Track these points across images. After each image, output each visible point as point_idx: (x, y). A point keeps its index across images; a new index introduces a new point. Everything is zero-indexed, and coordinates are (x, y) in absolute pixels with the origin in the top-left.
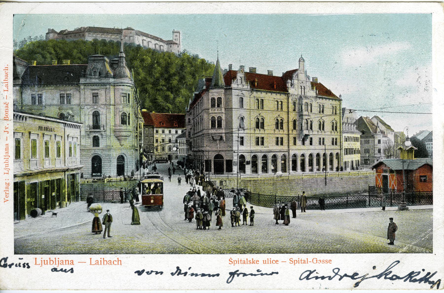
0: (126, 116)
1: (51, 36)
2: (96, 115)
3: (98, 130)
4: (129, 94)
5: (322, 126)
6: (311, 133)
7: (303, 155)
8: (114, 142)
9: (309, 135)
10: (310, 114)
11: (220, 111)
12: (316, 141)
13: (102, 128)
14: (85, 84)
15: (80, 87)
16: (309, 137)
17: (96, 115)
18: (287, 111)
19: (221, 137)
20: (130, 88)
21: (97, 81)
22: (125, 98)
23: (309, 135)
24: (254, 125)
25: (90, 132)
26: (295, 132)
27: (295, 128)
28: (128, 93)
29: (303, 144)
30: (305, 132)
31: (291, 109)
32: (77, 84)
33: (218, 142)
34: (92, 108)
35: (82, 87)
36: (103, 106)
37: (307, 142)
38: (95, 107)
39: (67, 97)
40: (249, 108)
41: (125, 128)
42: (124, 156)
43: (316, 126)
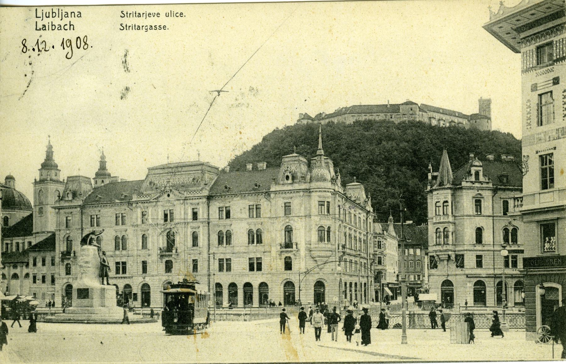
0: (324, 230)
1: (305, 122)
2: (289, 230)
3: (289, 249)
4: (328, 202)
11: (447, 220)
13: (294, 246)
14: (275, 192)
15: (270, 196)
17: (289, 230)
19: (449, 257)
21: (290, 188)
22: (323, 207)
24: (500, 238)
25: (282, 252)
32: (266, 192)
33: (446, 262)
34: (283, 222)
35: (272, 195)
36: (296, 219)
38: (287, 221)
39: (256, 208)
40: (491, 214)
41: (324, 246)
42: (322, 281)
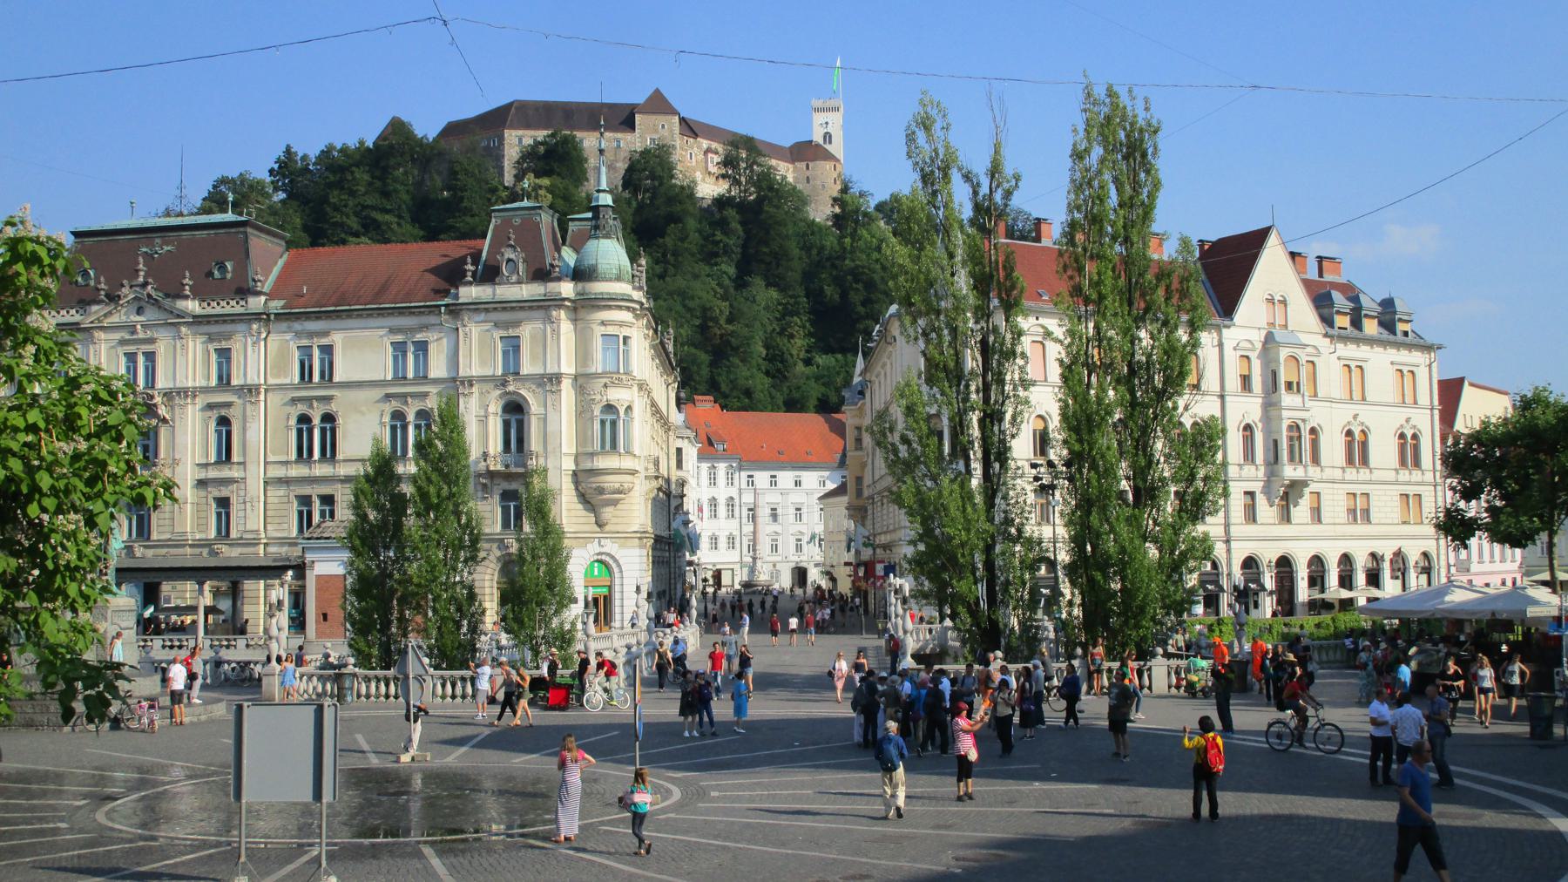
4: (626, 339)
5: (1357, 450)
6: (1313, 472)
7: (1284, 565)
9: (1304, 484)
10: (1309, 404)
12: (1335, 505)
16: (1307, 491)
18: (1217, 389)
20: (627, 316)
23: (1304, 484)
26: (1249, 470)
27: (1249, 455)
28: (625, 332)
29: (1286, 518)
30: (1290, 472)
31: (1233, 383)
37: (1301, 511)
43: (1333, 448)
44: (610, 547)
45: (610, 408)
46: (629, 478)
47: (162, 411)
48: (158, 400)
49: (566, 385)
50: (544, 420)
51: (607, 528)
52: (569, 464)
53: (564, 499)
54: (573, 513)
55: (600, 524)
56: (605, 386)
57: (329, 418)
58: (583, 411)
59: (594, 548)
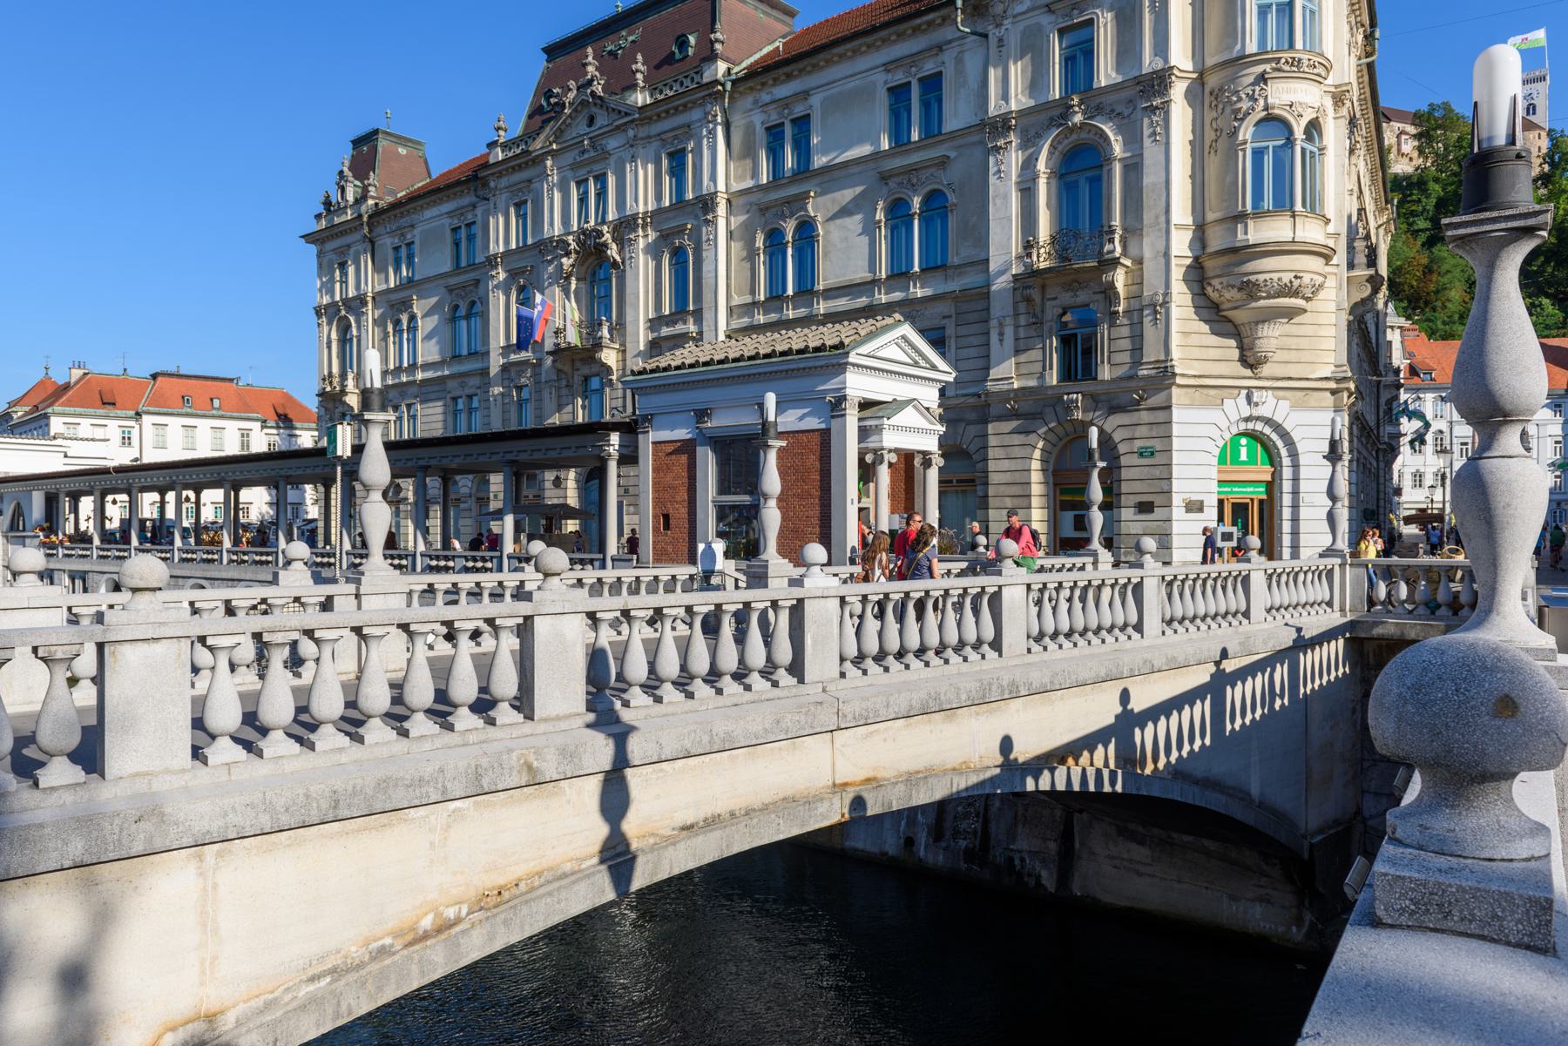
2: (1082, 169)
8: (1189, 342)
44: (1269, 405)
45: (1274, 122)
46: (1315, 263)
47: (613, 252)
48: (607, 237)
49: (1178, 90)
50: (1134, 168)
51: (1266, 370)
52: (1181, 245)
53: (1175, 312)
54: (1195, 339)
55: (1250, 359)
56: (1262, 78)
57: (806, 230)
58: (1214, 143)
59: (1236, 408)
